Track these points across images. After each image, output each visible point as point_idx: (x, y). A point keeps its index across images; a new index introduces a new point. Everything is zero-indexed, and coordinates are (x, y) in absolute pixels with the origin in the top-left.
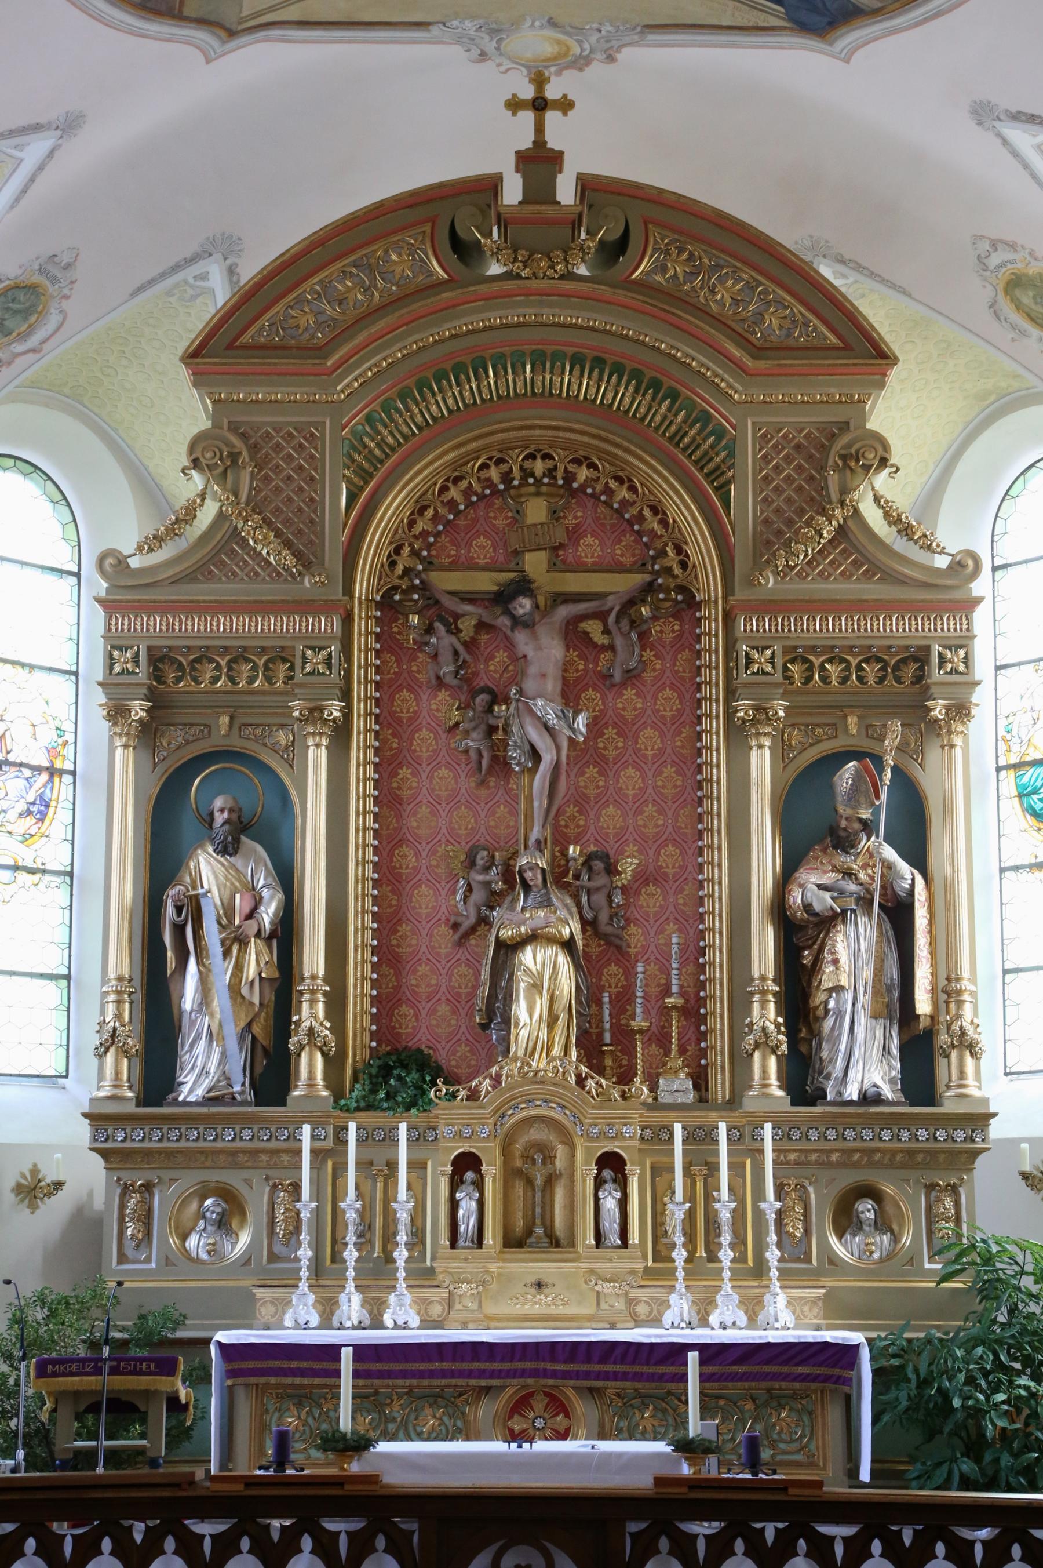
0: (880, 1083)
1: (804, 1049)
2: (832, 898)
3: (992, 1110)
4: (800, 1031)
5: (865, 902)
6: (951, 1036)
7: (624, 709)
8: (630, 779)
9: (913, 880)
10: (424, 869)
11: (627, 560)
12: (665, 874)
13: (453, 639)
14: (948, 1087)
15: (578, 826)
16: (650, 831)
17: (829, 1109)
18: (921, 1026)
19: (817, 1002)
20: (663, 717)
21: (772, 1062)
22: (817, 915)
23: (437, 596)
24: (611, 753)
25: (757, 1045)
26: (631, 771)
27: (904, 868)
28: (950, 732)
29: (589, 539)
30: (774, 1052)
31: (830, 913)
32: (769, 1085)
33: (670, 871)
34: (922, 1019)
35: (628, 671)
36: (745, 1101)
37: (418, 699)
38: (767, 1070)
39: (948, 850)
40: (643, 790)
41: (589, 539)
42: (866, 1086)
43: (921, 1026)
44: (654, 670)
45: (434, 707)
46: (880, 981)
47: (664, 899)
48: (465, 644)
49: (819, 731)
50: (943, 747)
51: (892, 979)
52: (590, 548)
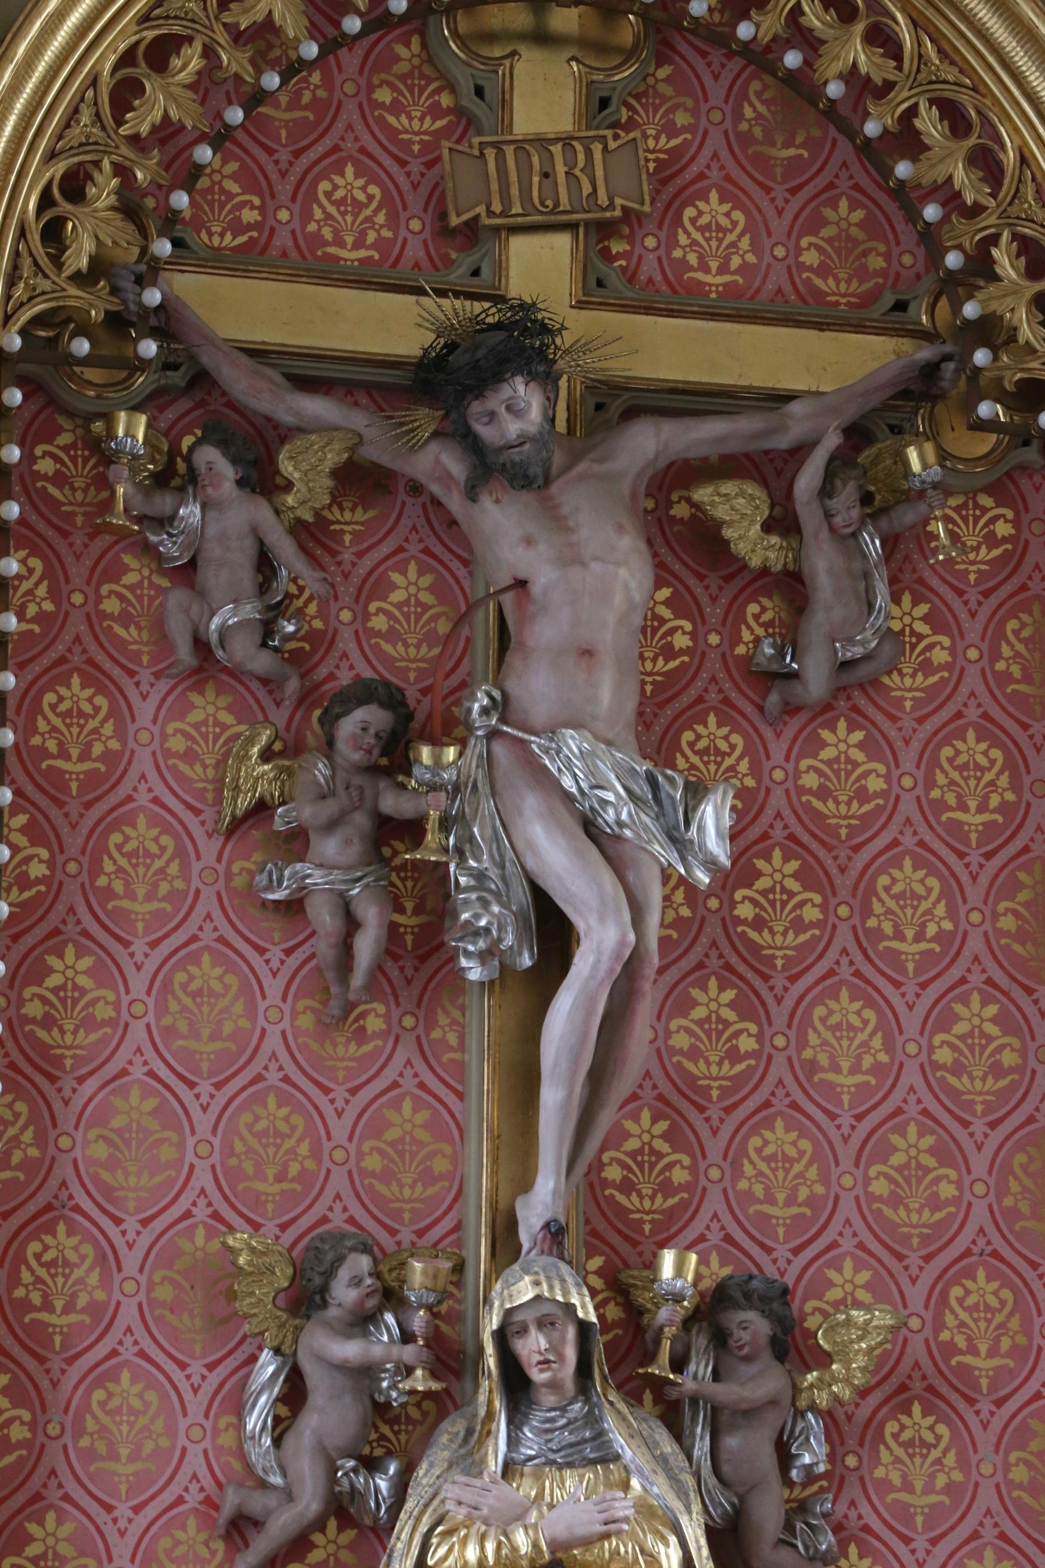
7: (823, 793)
8: (844, 1041)
10: (129, 1314)
11: (840, 289)
12: (965, 1372)
13: (261, 512)
15: (666, 1188)
16: (914, 1218)
20: (956, 826)
23: (208, 359)
24: (780, 942)
26: (846, 1007)
29: (713, 207)
33: (982, 1364)
35: (846, 665)
37: (121, 715)
40: (889, 1074)
41: (713, 207)
44: (926, 667)
45: (177, 744)
47: (963, 1463)
48: (298, 530)
52: (715, 239)
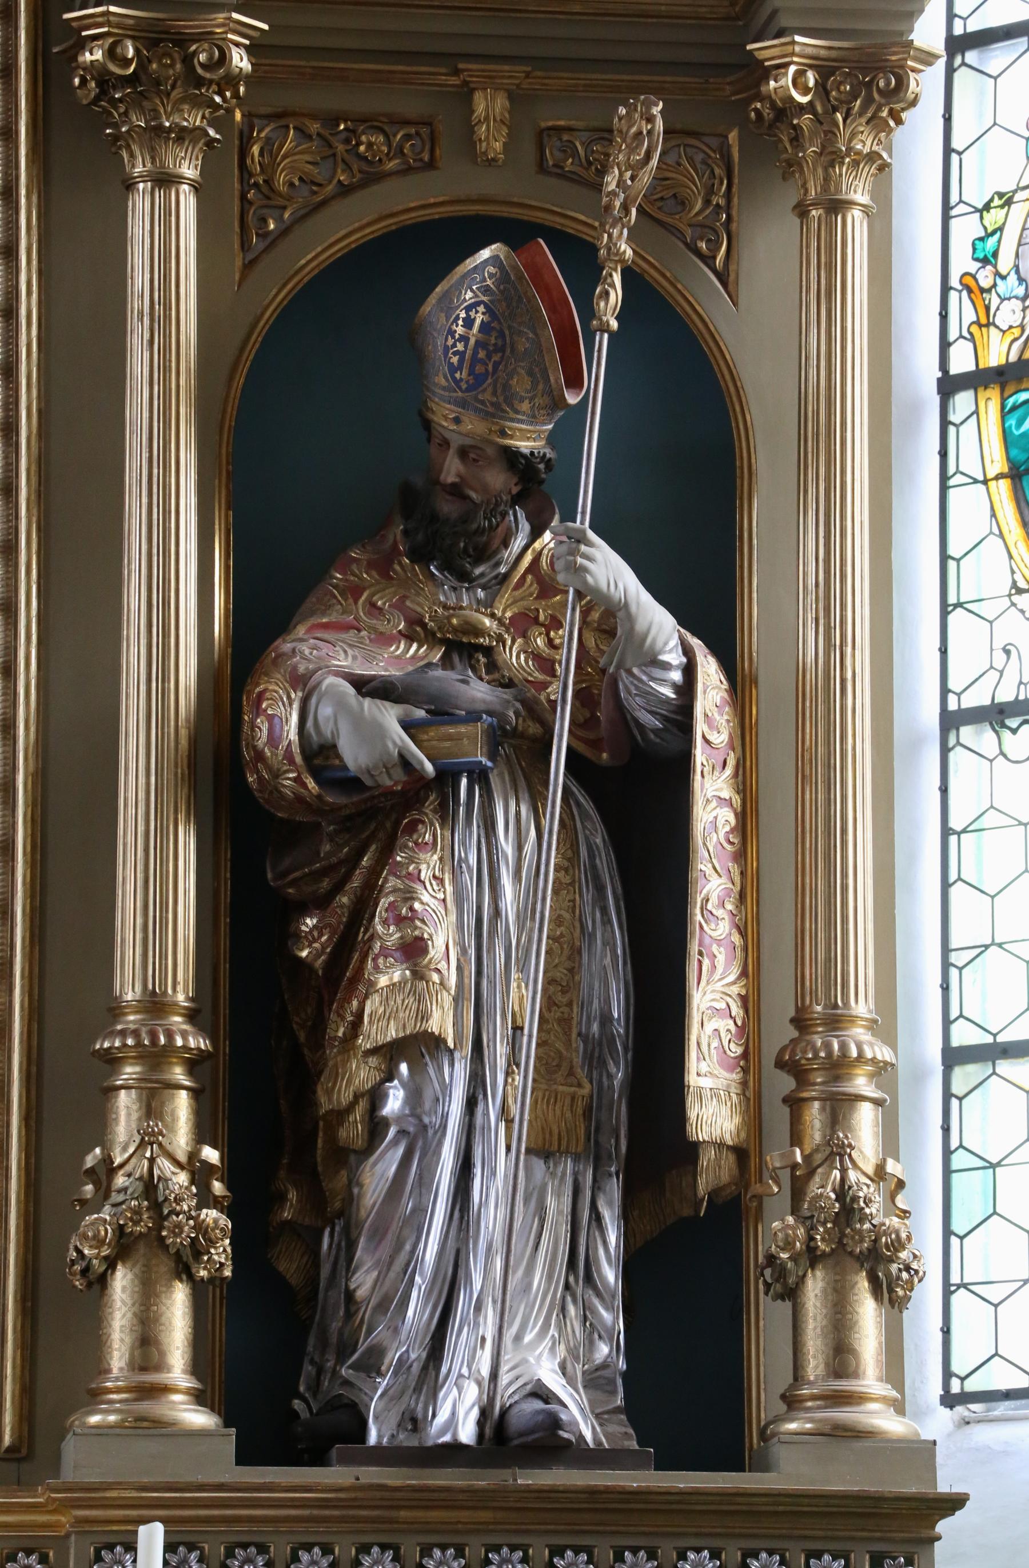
0: (555, 1383)
1: (289, 1266)
2: (408, 726)
3: (944, 1486)
4: (281, 1198)
5: (521, 748)
6: (809, 1222)
9: (689, 670)
14: (792, 1402)
17: (371, 1475)
18: (703, 1186)
19: (345, 1097)
21: (177, 1306)
22: (352, 784)
25: (124, 1247)
27: (659, 623)
28: (831, 157)
30: (183, 1270)
31: (393, 781)
32: (167, 1389)
34: (707, 1158)
36: (70, 1448)
38: (158, 1333)
39: (811, 571)
42: (508, 1389)
43: (703, 1186)
46: (565, 1022)
49: (370, 141)
50: (802, 211)
51: (606, 1019)
